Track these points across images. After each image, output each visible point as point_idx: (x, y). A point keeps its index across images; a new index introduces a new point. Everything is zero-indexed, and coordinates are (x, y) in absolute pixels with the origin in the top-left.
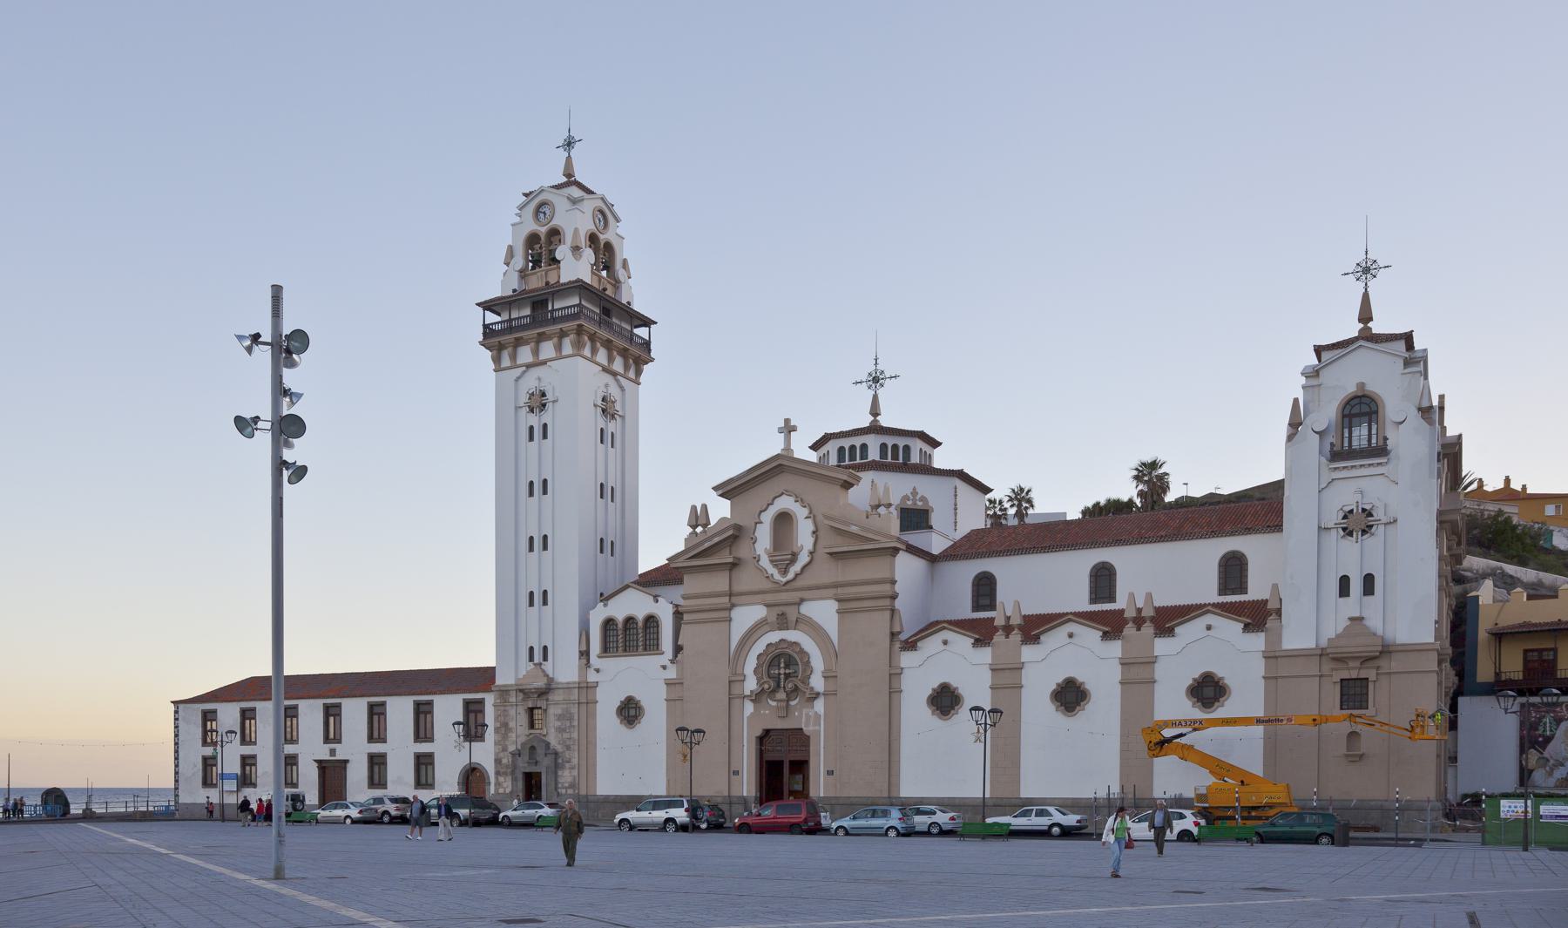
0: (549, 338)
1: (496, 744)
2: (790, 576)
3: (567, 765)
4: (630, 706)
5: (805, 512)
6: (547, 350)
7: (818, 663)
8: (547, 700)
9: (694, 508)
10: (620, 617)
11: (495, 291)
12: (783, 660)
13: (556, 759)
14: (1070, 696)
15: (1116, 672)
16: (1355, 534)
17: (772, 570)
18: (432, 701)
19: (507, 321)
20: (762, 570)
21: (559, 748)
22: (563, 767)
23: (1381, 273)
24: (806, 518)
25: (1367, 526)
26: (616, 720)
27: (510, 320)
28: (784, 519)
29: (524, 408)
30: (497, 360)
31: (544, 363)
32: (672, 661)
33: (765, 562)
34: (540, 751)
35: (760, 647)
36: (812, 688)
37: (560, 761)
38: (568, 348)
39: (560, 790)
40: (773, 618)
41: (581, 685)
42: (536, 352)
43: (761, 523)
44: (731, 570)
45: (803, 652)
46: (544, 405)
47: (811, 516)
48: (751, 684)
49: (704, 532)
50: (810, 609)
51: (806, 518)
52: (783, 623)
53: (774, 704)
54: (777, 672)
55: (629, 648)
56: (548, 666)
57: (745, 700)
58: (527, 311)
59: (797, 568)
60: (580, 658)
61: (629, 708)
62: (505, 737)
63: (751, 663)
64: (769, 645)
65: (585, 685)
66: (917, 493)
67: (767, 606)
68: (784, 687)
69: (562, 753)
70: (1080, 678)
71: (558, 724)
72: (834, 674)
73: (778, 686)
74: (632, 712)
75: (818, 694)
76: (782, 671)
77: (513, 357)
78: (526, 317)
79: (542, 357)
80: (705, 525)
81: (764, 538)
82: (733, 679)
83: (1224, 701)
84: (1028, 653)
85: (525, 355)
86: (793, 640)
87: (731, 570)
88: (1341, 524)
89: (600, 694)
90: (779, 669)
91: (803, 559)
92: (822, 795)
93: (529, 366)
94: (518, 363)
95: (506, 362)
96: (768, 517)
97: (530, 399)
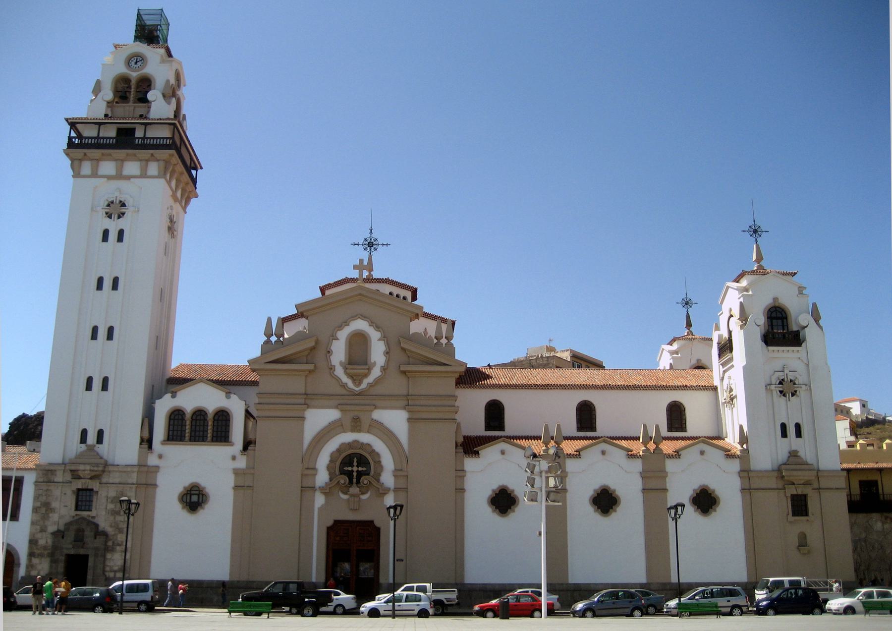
1: (33, 523)
2: (364, 385)
3: (118, 548)
4: (193, 492)
6: (132, 168)
7: (388, 461)
9: (269, 320)
11: (81, 113)
13: (106, 542)
15: (638, 483)
17: (345, 379)
19: (95, 138)
20: (338, 379)
21: (110, 530)
22: (112, 550)
23: (758, 223)
24: (379, 340)
26: (177, 507)
27: (98, 137)
31: (128, 178)
33: (340, 372)
34: (88, 533)
35: (333, 445)
37: (110, 543)
38: (153, 168)
39: (107, 574)
42: (120, 169)
43: (337, 339)
44: (306, 376)
45: (373, 452)
46: (123, 214)
47: (384, 338)
48: (322, 477)
50: (380, 415)
51: (379, 340)
52: (356, 425)
54: (350, 469)
56: (103, 449)
58: (113, 134)
59: (370, 379)
60: (141, 444)
61: (191, 495)
62: (45, 517)
63: (323, 460)
66: (427, 333)
69: (114, 535)
71: (111, 506)
72: (403, 474)
74: (195, 498)
75: (388, 490)
76: (355, 469)
78: (113, 138)
81: (339, 352)
85: (108, 167)
87: (306, 376)
91: (376, 373)
93: (110, 178)
96: (343, 335)
97: (109, 205)
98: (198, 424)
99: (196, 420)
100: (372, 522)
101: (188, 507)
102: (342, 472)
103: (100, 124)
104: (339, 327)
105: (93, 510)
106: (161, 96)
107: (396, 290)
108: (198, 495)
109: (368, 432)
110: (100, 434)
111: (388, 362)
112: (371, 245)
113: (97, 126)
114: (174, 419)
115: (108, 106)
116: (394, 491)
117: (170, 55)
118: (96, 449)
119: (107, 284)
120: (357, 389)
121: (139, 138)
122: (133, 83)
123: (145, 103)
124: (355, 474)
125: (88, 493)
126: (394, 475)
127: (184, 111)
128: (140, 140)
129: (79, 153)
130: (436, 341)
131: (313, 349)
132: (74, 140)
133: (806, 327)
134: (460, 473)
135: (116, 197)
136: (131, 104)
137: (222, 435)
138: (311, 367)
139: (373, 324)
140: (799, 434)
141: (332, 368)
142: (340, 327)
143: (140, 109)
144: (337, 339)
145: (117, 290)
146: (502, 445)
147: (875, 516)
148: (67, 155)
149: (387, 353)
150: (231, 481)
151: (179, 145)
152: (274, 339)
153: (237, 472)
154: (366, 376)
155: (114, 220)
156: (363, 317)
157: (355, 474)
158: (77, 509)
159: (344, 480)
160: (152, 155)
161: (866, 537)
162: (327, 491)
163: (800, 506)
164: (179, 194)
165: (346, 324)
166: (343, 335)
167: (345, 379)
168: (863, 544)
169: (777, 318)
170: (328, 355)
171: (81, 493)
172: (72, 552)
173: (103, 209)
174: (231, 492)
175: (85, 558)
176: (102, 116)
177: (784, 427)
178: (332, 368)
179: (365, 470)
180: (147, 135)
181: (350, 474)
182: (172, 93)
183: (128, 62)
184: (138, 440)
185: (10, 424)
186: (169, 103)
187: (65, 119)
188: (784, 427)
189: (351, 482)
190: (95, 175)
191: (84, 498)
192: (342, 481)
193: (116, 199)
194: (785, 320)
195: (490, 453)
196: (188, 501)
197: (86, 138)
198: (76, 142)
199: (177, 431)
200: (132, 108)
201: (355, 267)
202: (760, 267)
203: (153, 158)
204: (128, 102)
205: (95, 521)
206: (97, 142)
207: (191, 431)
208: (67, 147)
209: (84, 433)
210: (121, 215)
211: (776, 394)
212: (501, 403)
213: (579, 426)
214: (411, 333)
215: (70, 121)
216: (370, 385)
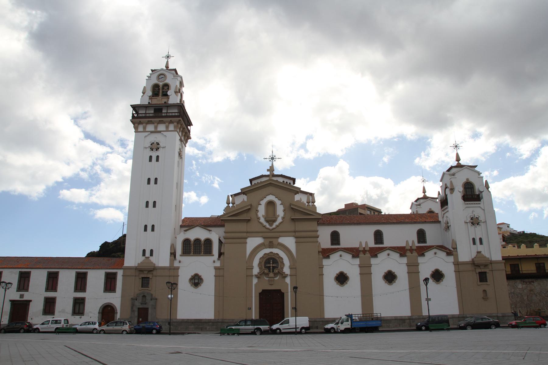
0: (164, 123)
2: (274, 226)
4: (196, 278)
5: (280, 202)
6: (161, 127)
8: (152, 274)
11: (138, 102)
12: (271, 261)
14: (390, 277)
16: (475, 225)
17: (265, 223)
18: (87, 272)
19: (144, 114)
20: (261, 223)
25: (474, 224)
26: (189, 285)
27: (146, 113)
28: (271, 204)
29: (148, 149)
31: (160, 132)
33: (262, 220)
34: (148, 298)
35: (261, 254)
36: (284, 273)
40: (267, 243)
41: (171, 268)
42: (156, 128)
43: (261, 204)
46: (158, 148)
48: (256, 270)
50: (282, 240)
52: (271, 246)
53: (267, 279)
54: (269, 265)
56: (153, 259)
59: (277, 223)
60: (170, 256)
61: (195, 279)
63: (256, 262)
64: (265, 254)
65: (173, 268)
66: (302, 200)
67: (264, 238)
70: (441, 269)
72: (295, 267)
73: (270, 271)
74: (196, 281)
75: (288, 275)
76: (271, 265)
77: (145, 128)
78: (152, 113)
79: (159, 129)
81: (262, 210)
83: (435, 282)
84: (373, 261)
85: (150, 128)
86: (275, 253)
88: (471, 221)
89: (180, 272)
90: (270, 264)
91: (279, 220)
93: (152, 132)
94: (147, 130)
96: (263, 202)
97: (151, 145)
100: (280, 290)
101: (193, 285)
102: (266, 267)
106: (174, 92)
107: (286, 180)
109: (276, 248)
110: (152, 251)
111: (285, 215)
113: (145, 108)
114: (186, 244)
115: (150, 99)
116: (290, 275)
117: (177, 73)
119: (152, 181)
120: (271, 228)
121: (164, 113)
122: (161, 87)
123: (166, 96)
124: (271, 267)
125: (147, 279)
127: (184, 99)
128: (165, 114)
130: (307, 204)
131: (249, 209)
132: (135, 115)
133: (483, 192)
134: (321, 267)
135: (155, 141)
136: (160, 96)
137: (208, 251)
140: (481, 243)
141: (258, 218)
143: (164, 100)
145: (157, 184)
146: (340, 253)
147: (518, 281)
148: (131, 121)
149: (284, 210)
150: (213, 272)
151: (183, 115)
153: (216, 268)
154: (275, 221)
157: (271, 267)
158: (142, 287)
159: (266, 271)
161: (514, 292)
162: (257, 277)
163: (483, 277)
164: (183, 138)
166: (263, 202)
167: (265, 223)
168: (513, 294)
169: (468, 188)
170: (257, 212)
171: (143, 279)
172: (141, 307)
175: (147, 309)
176: (147, 104)
177: (474, 240)
178: (259, 218)
179: (276, 266)
180: (168, 112)
181: (269, 268)
182: (179, 92)
183: (158, 77)
184: (169, 254)
185: (100, 246)
186: (177, 95)
187: (130, 105)
188: (474, 240)
189: (270, 271)
191: (145, 282)
192: (266, 271)
194: (472, 189)
195: (335, 257)
196: (193, 282)
197: (140, 114)
198: (136, 116)
199: (187, 249)
202: (459, 164)
203: (171, 122)
204: (159, 96)
208: (131, 118)
209: (144, 251)
210: (157, 149)
211: (470, 225)
212: (338, 232)
213: (376, 242)
214: (295, 201)
215: (133, 106)
216: (277, 226)
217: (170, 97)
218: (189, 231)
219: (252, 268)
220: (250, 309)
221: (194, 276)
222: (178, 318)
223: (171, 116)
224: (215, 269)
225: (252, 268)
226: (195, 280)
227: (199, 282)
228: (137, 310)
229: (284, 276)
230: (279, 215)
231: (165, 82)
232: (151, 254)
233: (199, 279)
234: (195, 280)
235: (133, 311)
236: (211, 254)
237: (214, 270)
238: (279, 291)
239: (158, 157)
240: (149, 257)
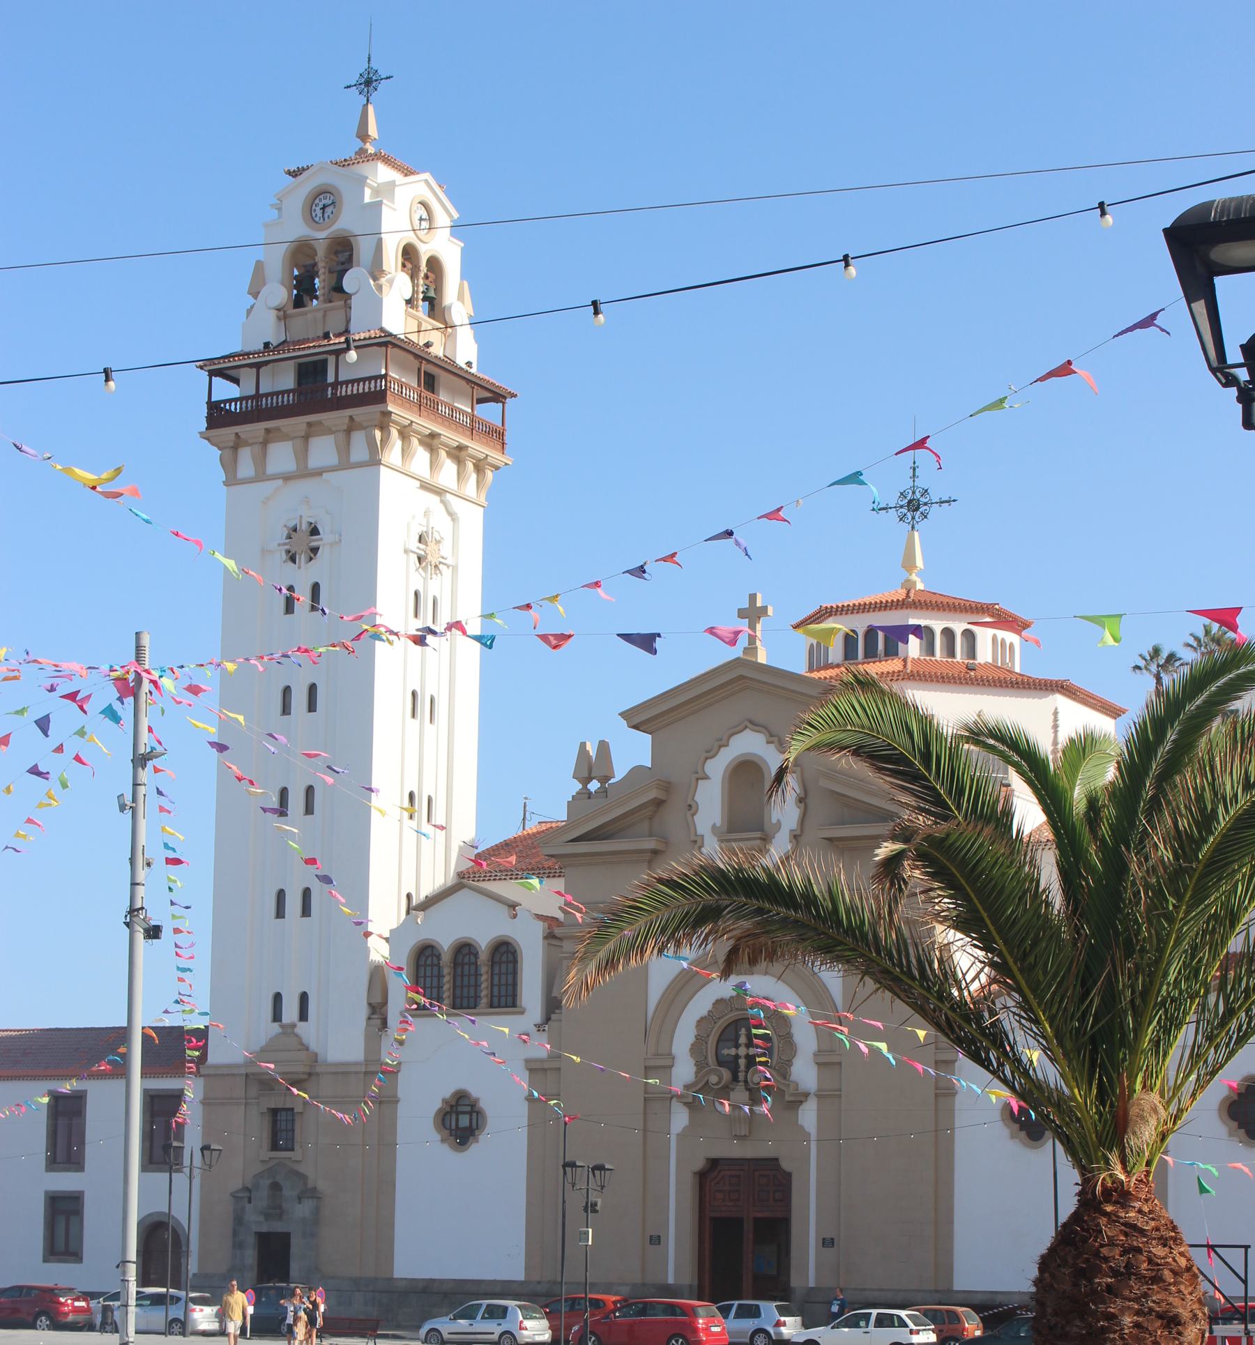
0: (329, 431)
4: (461, 1109)
6: (323, 450)
10: (446, 943)
26: (433, 1135)
27: (257, 396)
30: (230, 465)
31: (318, 473)
32: (539, 1027)
35: (701, 1004)
42: (302, 455)
43: (706, 777)
46: (315, 550)
48: (684, 1072)
49: (603, 792)
54: (733, 1051)
55: (464, 1001)
57: (674, 1100)
68: (746, 1082)
73: (735, 1078)
74: (464, 1121)
75: (806, 1095)
76: (742, 1051)
77: (261, 461)
78: (288, 392)
79: (314, 461)
80: (604, 779)
82: (652, 1063)
85: (281, 456)
87: (650, 862)
89: (405, 1086)
90: (737, 1046)
92: (812, 1284)
93: (287, 478)
95: (246, 467)
96: (717, 767)
97: (289, 537)
98: (466, 972)
99: (463, 965)
103: (258, 366)
104: (707, 752)
105: (297, 1147)
108: (458, 1113)
110: (304, 998)
112: (913, 506)
113: (254, 370)
116: (819, 1096)
118: (297, 1030)
124: (742, 1062)
126: (816, 1063)
129: (228, 433)
131: (658, 803)
135: (301, 517)
138: (650, 844)
139: (772, 739)
141: (695, 842)
142: (711, 754)
144: (706, 777)
152: (594, 786)
155: (299, 568)
156: (755, 725)
157: (742, 1062)
158: (275, 1147)
160: (351, 417)
165: (720, 743)
166: (717, 767)
170: (689, 813)
172: (264, 1229)
173: (279, 545)
174: (523, 1109)
175: (285, 1239)
181: (731, 1064)
189: (735, 1078)
190: (262, 476)
193: (301, 523)
196: (453, 1126)
200: (320, 315)
201: (742, 614)
205: (301, 1168)
206: (257, 405)
207: (455, 987)
209: (278, 998)
217: (354, 301)
218: (439, 904)
219: (663, 1066)
220: (656, 1240)
221: (453, 1103)
222: (397, 1275)
223: (370, 392)
224: (531, 1070)
225: (667, 1062)
226: (460, 1116)
227: (474, 1126)
228: (251, 1240)
229: (788, 1098)
230: (779, 822)
231: (332, 229)
232: (303, 1016)
233: (474, 1115)
234: (460, 1116)
235: (238, 1245)
236: (514, 1005)
237: (527, 1073)
238: (772, 1163)
239: (316, 589)
240: (294, 1026)
